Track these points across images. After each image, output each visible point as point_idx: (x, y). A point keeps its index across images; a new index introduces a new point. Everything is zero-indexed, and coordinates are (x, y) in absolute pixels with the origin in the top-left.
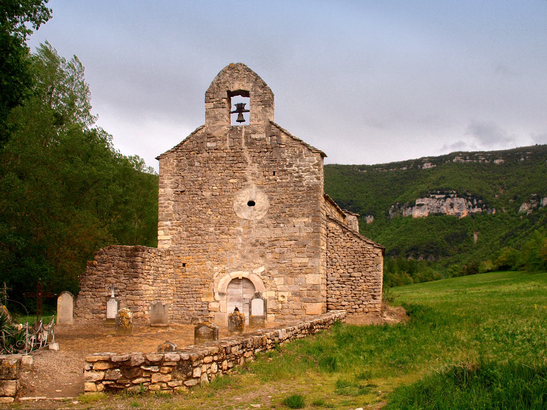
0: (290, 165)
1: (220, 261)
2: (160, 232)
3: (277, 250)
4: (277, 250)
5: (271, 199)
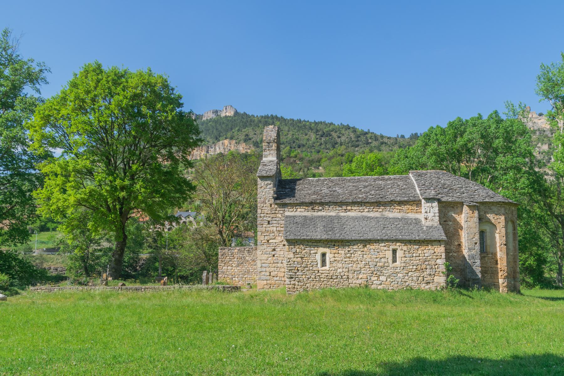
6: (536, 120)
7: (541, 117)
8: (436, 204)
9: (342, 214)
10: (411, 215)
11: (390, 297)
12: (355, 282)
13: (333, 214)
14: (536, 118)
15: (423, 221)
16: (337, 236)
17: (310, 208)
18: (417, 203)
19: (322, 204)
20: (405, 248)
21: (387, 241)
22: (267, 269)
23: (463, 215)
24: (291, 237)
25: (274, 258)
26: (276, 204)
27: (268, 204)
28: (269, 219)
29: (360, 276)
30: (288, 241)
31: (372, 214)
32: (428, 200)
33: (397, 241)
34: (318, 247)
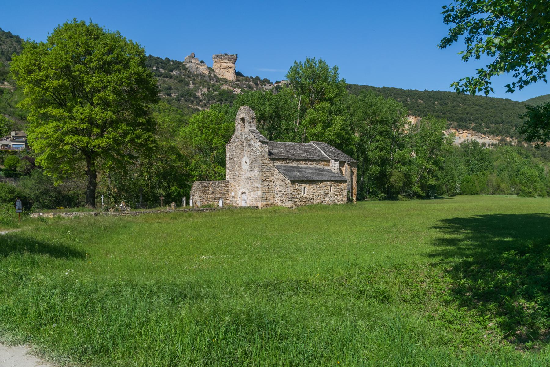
0: (254, 147)
1: (239, 185)
2: (227, 174)
3: (251, 181)
4: (251, 181)
5: (250, 161)
6: (199, 66)
7: (202, 64)
8: (338, 162)
9: (299, 166)
10: (326, 167)
11: (327, 207)
12: (317, 201)
13: (295, 165)
14: (199, 64)
15: (333, 171)
16: (309, 179)
17: (285, 162)
18: (328, 161)
19: (291, 160)
20: (335, 184)
21: (329, 181)
22: (265, 196)
23: (344, 168)
24: (292, 179)
25: (269, 189)
26: (270, 158)
27: (265, 158)
28: (266, 167)
29: (318, 199)
30: (291, 181)
31: (311, 166)
32: (336, 160)
33: (332, 181)
34: (303, 184)
